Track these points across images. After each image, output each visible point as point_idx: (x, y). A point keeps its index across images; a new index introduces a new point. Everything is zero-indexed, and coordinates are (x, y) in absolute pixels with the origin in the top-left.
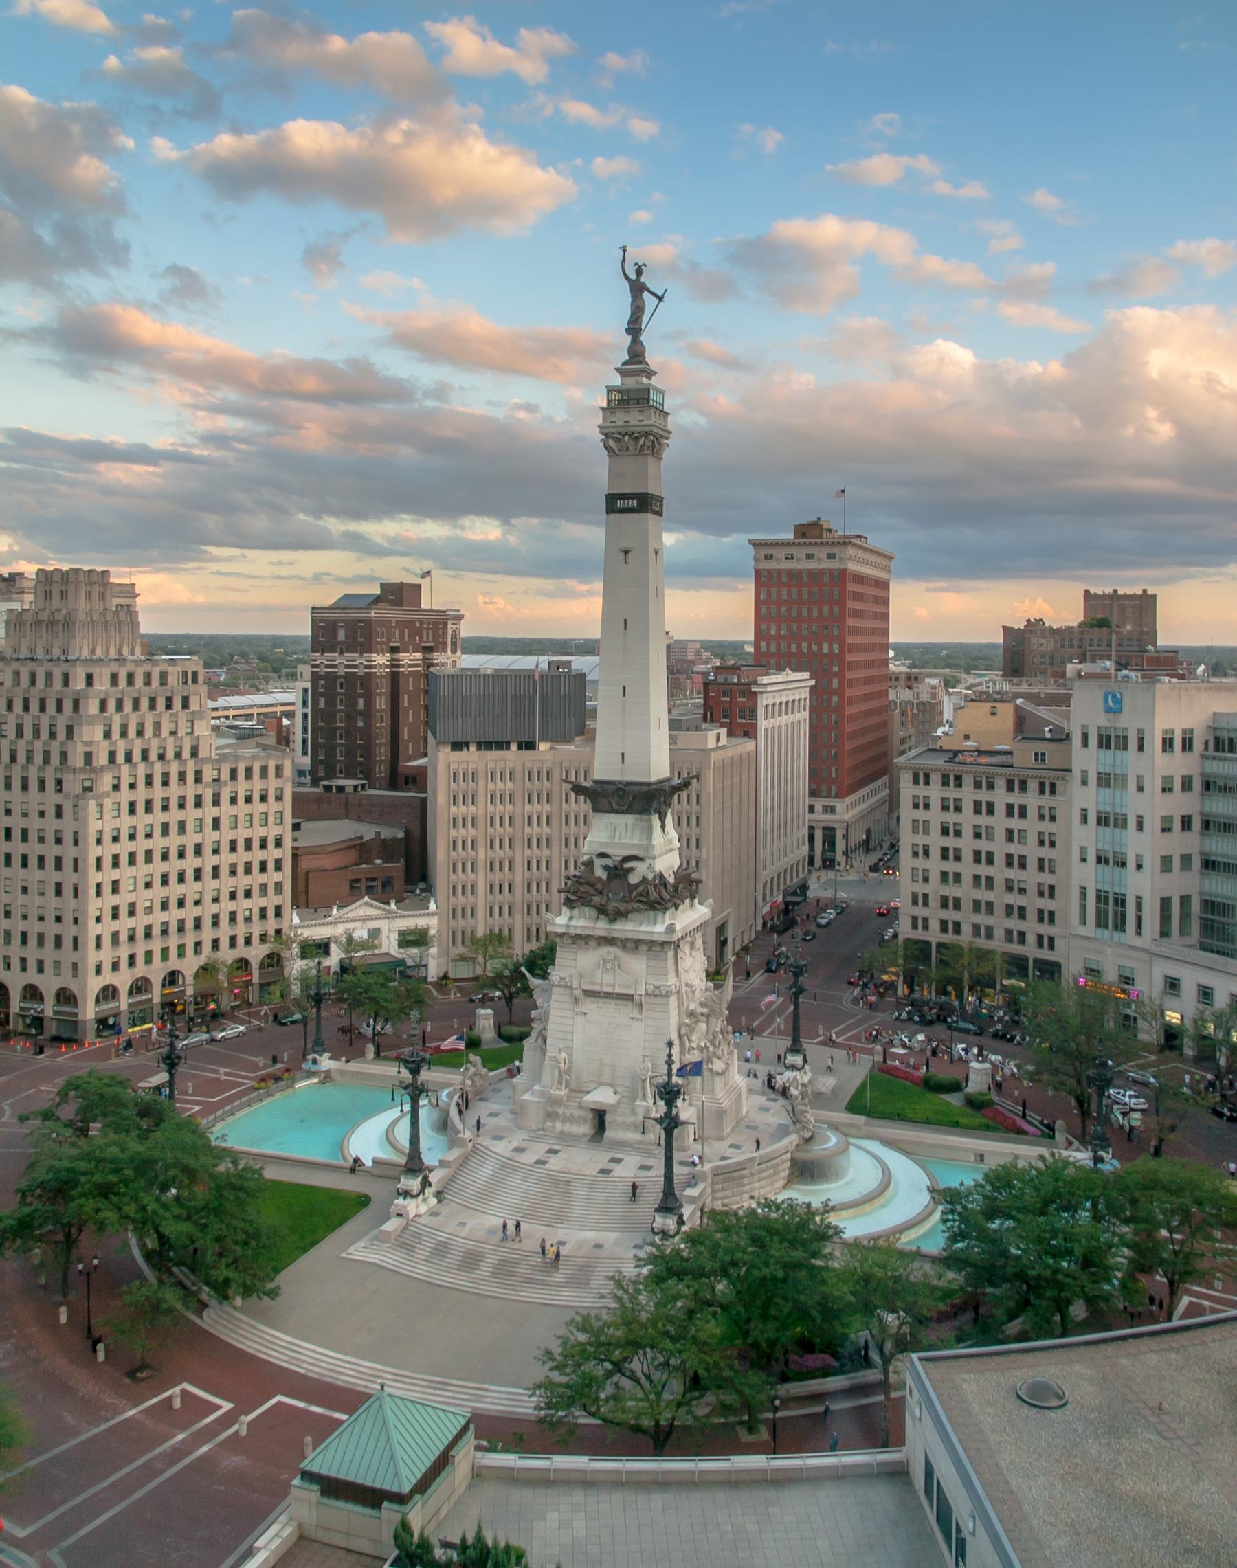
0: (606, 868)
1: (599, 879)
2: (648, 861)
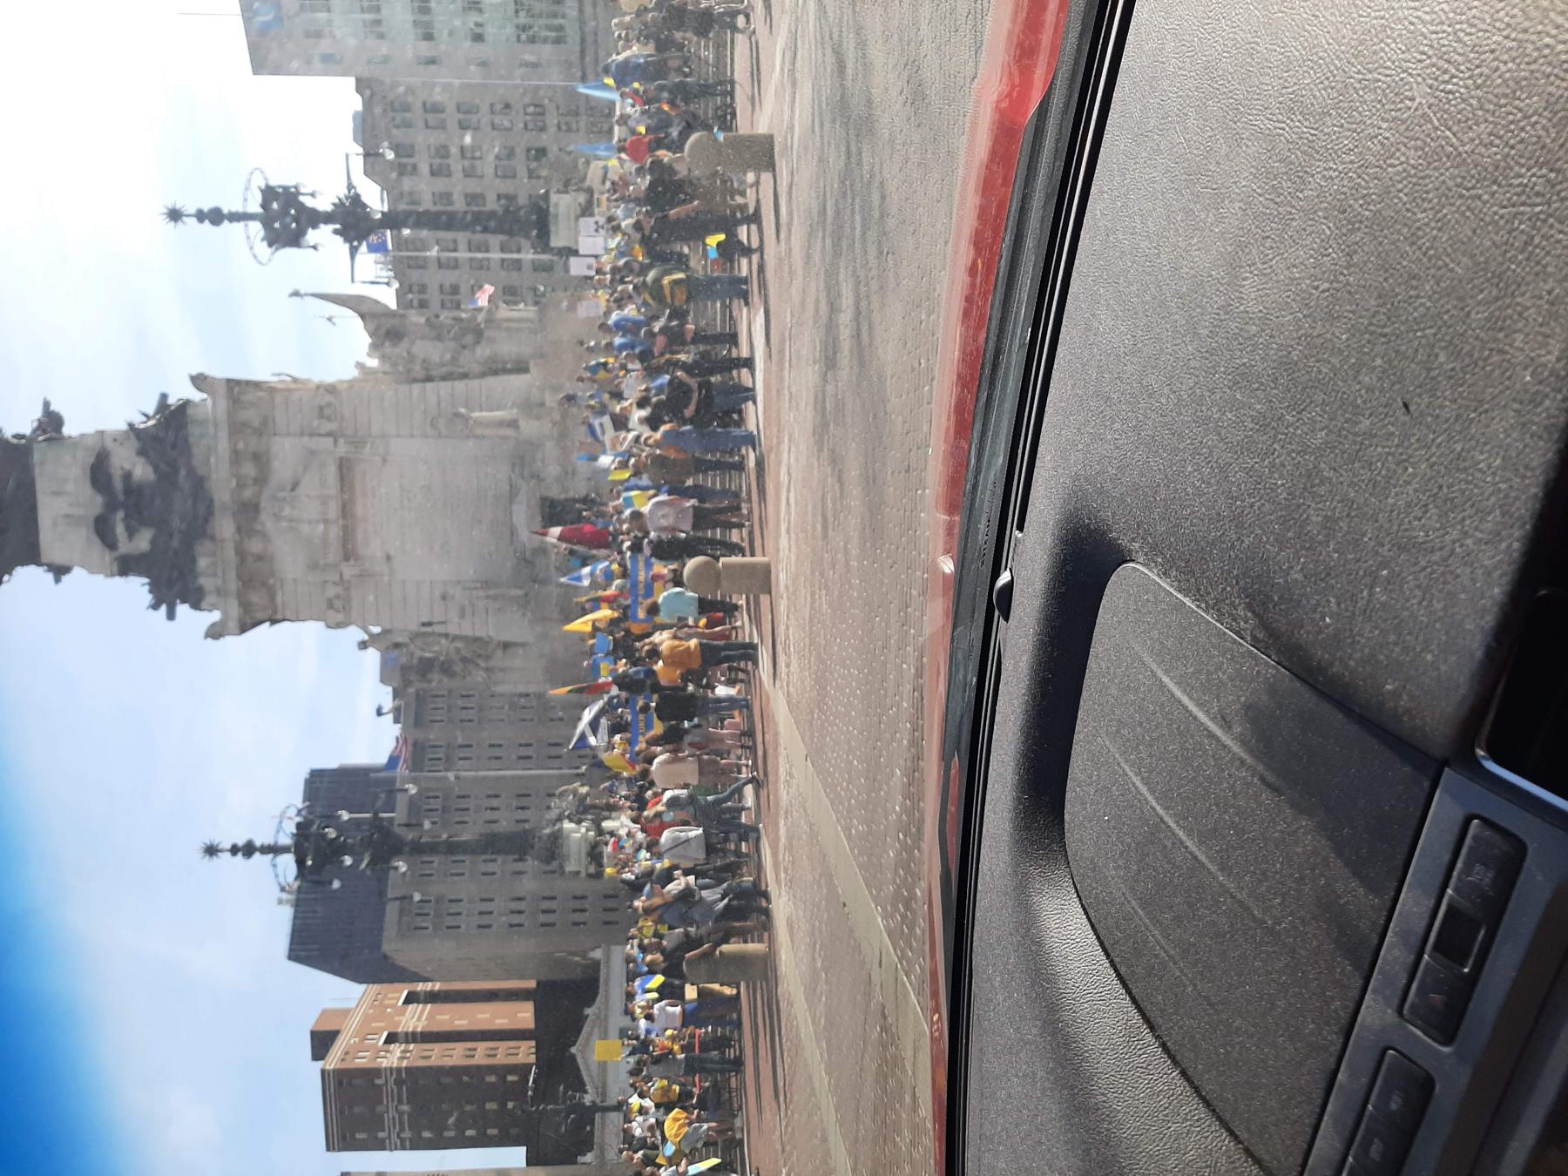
0: (131, 532)
1: (153, 542)
2: (109, 444)
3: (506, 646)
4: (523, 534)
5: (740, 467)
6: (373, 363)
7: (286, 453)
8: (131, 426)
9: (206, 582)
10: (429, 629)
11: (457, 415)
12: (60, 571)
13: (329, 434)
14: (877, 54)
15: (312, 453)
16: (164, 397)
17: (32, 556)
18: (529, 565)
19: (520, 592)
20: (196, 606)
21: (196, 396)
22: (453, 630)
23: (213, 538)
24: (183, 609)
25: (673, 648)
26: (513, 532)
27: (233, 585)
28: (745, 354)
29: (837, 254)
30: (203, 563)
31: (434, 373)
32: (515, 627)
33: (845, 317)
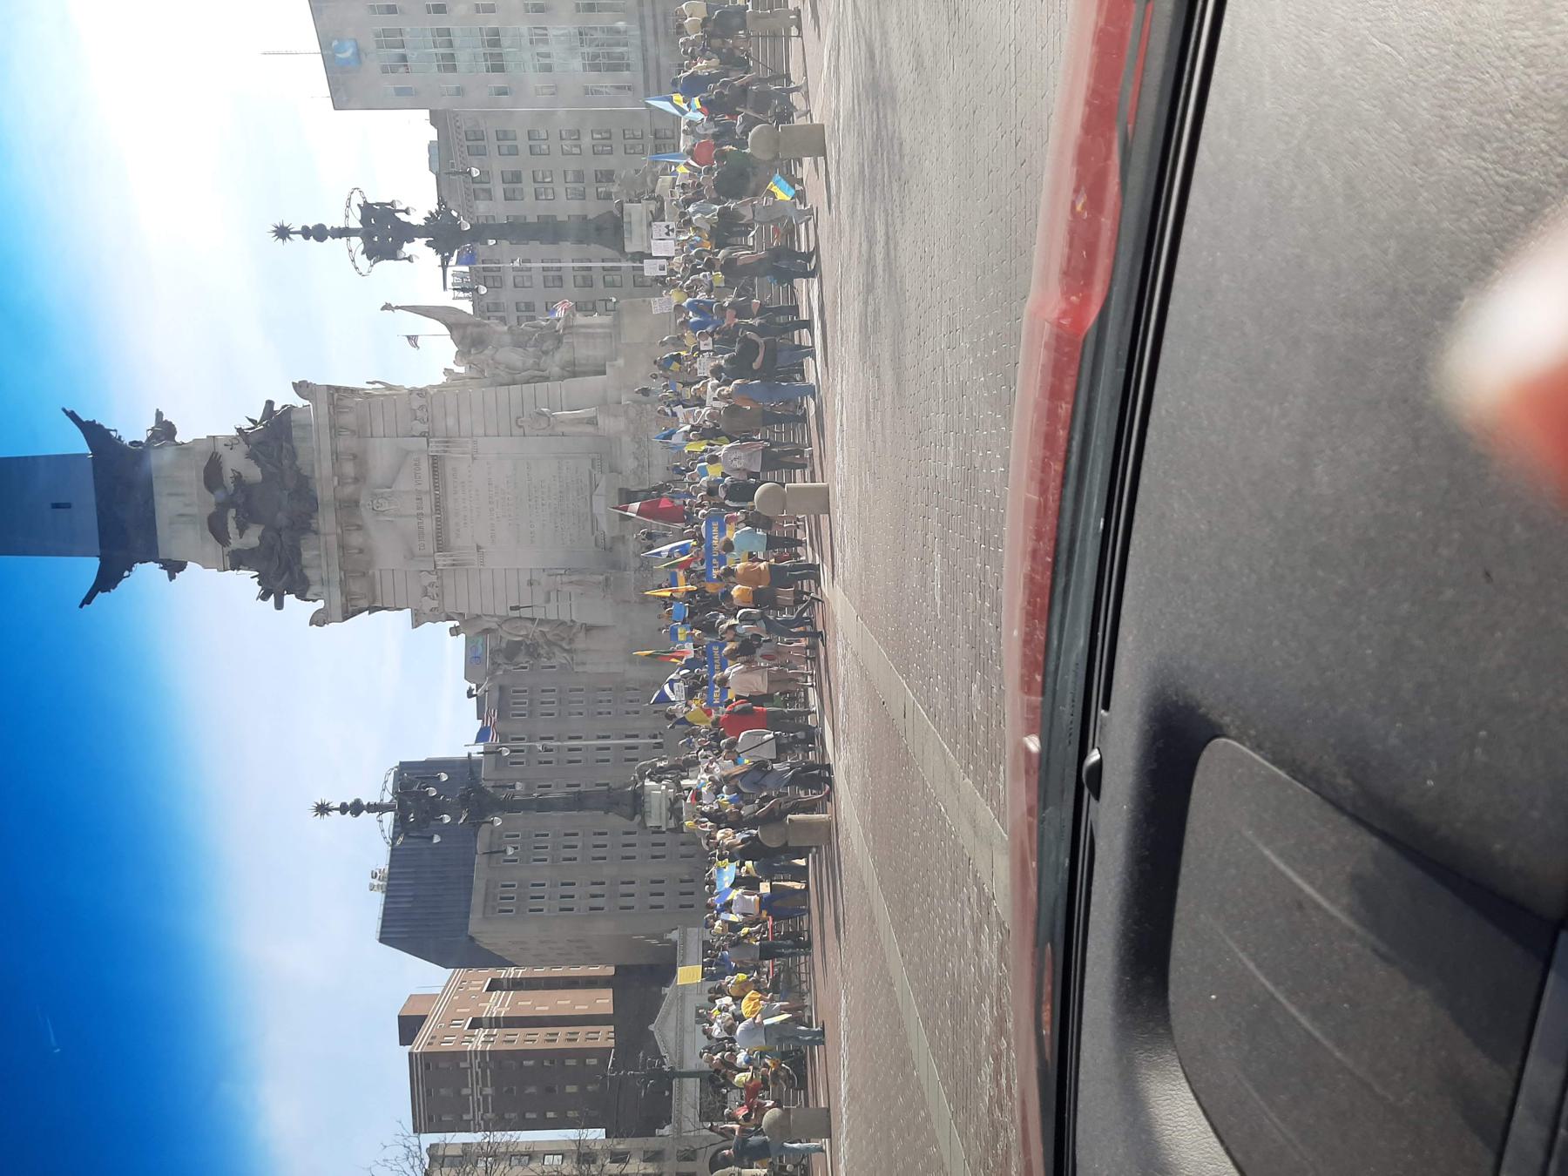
0: (242, 530)
1: (261, 538)
2: (221, 449)
3: (589, 629)
4: (604, 525)
5: (804, 418)
6: (461, 370)
7: (382, 454)
8: (239, 430)
9: (311, 574)
10: (516, 613)
11: (542, 414)
12: (174, 567)
13: (422, 435)
14: (894, 41)
15: (408, 453)
16: (270, 403)
17: (150, 554)
18: (609, 556)
19: (601, 578)
20: (302, 596)
21: (300, 402)
22: (539, 614)
23: (316, 533)
24: (289, 599)
25: (746, 569)
26: (594, 521)
27: (336, 576)
28: (804, 316)
29: (873, 200)
30: (307, 555)
31: (517, 377)
32: (594, 610)
33: (879, 249)
